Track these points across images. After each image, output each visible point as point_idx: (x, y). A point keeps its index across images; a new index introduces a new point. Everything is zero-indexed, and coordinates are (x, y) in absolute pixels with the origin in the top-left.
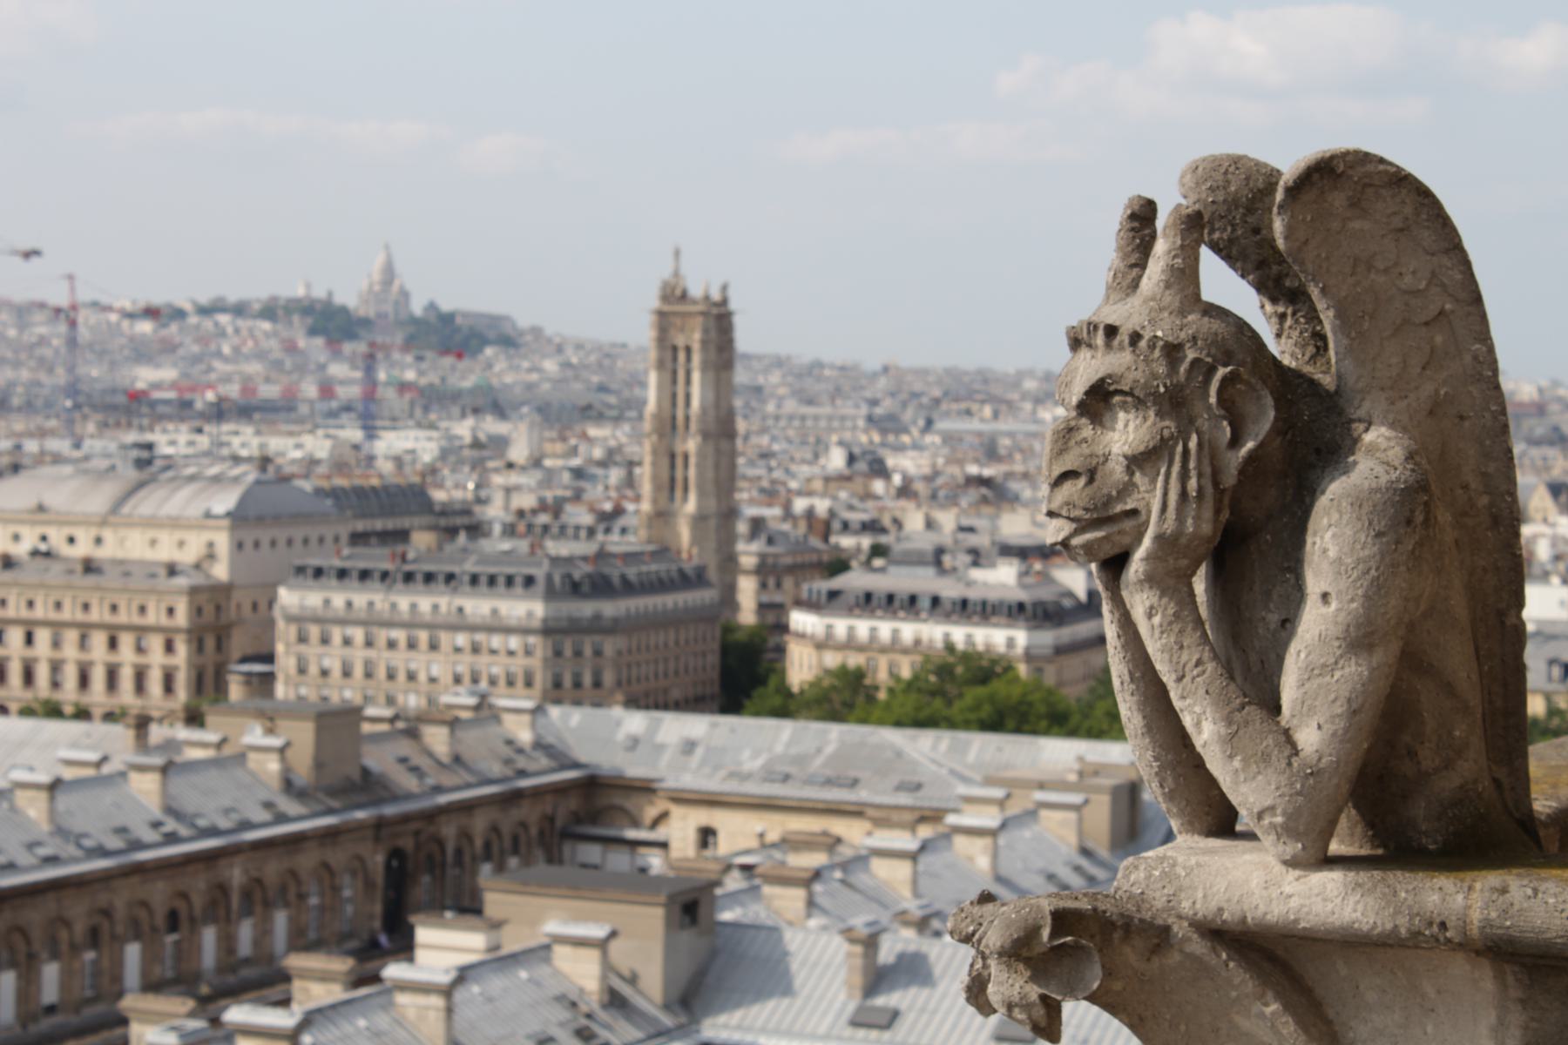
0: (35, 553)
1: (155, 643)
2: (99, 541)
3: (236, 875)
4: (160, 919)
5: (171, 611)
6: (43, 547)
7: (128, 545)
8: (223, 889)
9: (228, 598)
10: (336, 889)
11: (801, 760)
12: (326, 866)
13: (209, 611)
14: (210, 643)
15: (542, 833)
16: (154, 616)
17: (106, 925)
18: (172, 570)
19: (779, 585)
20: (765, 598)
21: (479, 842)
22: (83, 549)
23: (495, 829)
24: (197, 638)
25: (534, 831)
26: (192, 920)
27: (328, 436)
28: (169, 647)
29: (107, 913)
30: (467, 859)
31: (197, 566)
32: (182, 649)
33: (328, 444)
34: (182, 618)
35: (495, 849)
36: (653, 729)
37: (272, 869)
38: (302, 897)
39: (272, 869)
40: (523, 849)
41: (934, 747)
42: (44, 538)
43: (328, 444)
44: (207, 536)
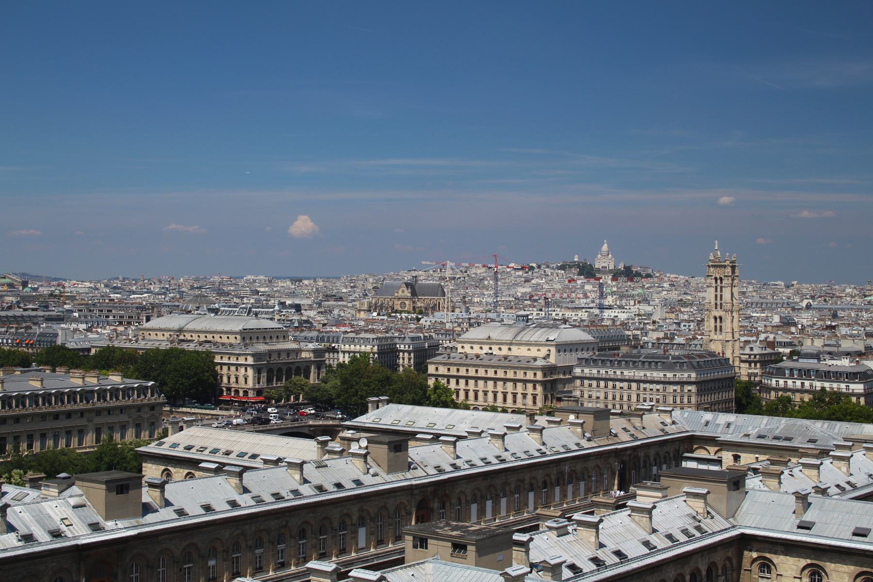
2: (510, 349)
3: (567, 469)
4: (540, 484)
6: (490, 352)
8: (562, 473)
10: (602, 474)
11: (770, 430)
12: (598, 466)
15: (674, 456)
17: (522, 485)
20: (750, 371)
21: (652, 458)
23: (658, 454)
25: (672, 455)
26: (551, 484)
27: (587, 312)
29: (522, 481)
30: (648, 465)
31: (544, 358)
35: (658, 461)
36: (715, 419)
37: (579, 467)
38: (590, 477)
39: (579, 467)
40: (668, 462)
41: (822, 427)
43: (587, 314)
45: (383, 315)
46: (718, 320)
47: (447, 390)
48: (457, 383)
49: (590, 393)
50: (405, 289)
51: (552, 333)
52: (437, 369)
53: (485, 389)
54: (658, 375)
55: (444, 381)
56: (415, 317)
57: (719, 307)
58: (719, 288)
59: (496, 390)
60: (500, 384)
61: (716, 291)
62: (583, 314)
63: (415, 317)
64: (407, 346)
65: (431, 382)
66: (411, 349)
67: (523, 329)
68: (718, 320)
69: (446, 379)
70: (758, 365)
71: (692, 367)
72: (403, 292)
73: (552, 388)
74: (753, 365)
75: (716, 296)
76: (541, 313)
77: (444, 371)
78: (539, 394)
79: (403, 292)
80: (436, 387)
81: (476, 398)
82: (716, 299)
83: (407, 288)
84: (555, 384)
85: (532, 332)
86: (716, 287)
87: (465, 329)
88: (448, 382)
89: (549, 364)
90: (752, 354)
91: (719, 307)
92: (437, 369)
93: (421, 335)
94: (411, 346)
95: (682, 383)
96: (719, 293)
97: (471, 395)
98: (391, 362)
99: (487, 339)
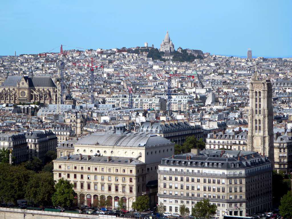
0: (96, 155)
1: (128, 179)
5: (131, 171)
6: (98, 154)
7: (120, 153)
9: (145, 167)
13: (140, 170)
14: (141, 179)
16: (127, 172)
18: (131, 160)
19: (284, 151)
20: (281, 155)
22: (108, 154)
24: (138, 178)
28: (131, 181)
31: (137, 159)
32: (134, 181)
33: (158, 99)
34: (134, 173)
42: (98, 151)
44: (139, 151)
45: (11, 107)
46: (258, 122)
47: (68, 182)
48: (75, 176)
49: (171, 185)
50: (24, 82)
51: (142, 141)
52: (60, 167)
53: (95, 181)
54: (220, 172)
55: (64, 176)
56: (34, 107)
57: (258, 112)
58: (258, 99)
59: (103, 182)
60: (106, 177)
61: (256, 101)
62: (156, 99)
63: (34, 107)
64: (33, 140)
65: (56, 178)
66: (36, 142)
67: (122, 137)
68: (258, 122)
69: (67, 175)
70: (286, 150)
71: (241, 166)
72: (23, 84)
73: (143, 180)
74: (282, 150)
75: (256, 105)
76: (125, 99)
77: (65, 169)
78: (134, 185)
79: (23, 84)
80: (62, 181)
81: (89, 187)
82: (256, 107)
83: (26, 81)
84: (146, 177)
85: (128, 140)
86: (256, 99)
87: (73, 121)
88: (69, 176)
89: (141, 163)
90: (282, 143)
91: (258, 112)
92: (60, 167)
93: (44, 131)
94: (37, 140)
95: (235, 177)
96: (258, 103)
97: (85, 186)
98: (21, 153)
99: (96, 145)
